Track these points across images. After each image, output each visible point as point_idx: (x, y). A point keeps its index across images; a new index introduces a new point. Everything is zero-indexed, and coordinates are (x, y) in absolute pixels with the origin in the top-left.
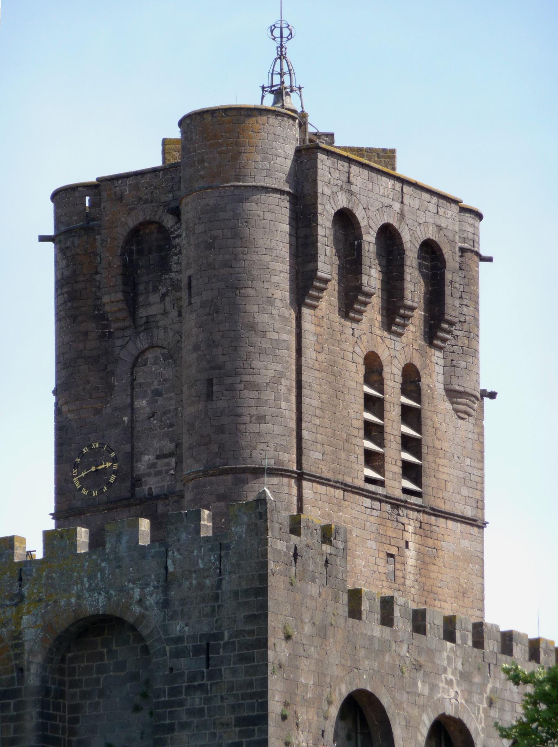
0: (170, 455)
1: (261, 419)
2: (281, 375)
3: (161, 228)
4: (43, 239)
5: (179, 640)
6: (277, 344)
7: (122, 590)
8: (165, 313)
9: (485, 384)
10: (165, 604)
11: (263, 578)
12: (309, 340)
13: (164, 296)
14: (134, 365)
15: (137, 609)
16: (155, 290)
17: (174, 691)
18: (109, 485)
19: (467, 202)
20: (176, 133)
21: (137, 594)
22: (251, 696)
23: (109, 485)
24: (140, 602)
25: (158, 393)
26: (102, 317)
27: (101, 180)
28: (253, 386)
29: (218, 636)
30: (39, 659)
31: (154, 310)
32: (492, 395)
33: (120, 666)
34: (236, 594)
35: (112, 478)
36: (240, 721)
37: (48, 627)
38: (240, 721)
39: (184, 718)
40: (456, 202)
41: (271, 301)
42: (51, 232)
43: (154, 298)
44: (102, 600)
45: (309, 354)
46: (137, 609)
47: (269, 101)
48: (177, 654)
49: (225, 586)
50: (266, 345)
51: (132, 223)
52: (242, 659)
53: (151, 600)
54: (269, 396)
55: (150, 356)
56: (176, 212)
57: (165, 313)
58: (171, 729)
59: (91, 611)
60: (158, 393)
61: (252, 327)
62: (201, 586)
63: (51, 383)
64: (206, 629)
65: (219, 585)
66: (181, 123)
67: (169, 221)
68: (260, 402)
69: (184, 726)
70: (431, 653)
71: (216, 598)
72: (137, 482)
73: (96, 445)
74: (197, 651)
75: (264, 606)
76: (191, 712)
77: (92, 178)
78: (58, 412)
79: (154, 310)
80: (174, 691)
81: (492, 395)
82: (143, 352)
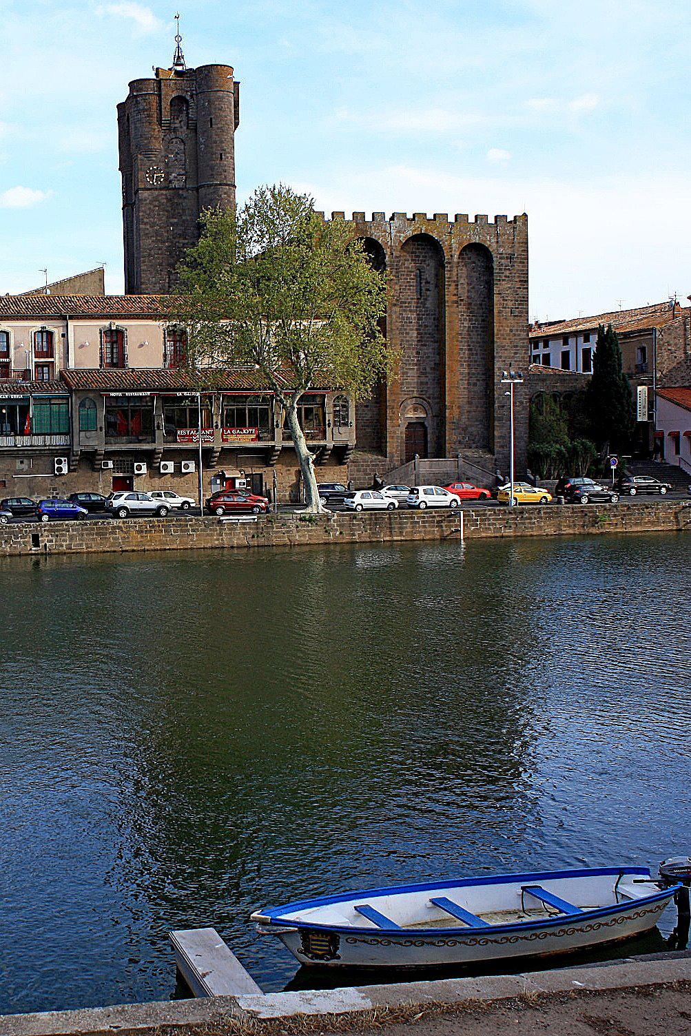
0: (182, 175)
5: (501, 254)
13: (180, 122)
16: (177, 119)
18: (161, 182)
22: (524, 274)
23: (161, 182)
30: (458, 253)
33: (469, 259)
34: (519, 243)
35: (162, 180)
36: (521, 281)
37: (460, 244)
38: (521, 281)
43: (177, 121)
48: (501, 258)
52: (520, 262)
53: (493, 241)
55: (174, 140)
59: (474, 241)
62: (508, 239)
69: (503, 280)
73: (155, 167)
76: (506, 276)
82: (173, 138)
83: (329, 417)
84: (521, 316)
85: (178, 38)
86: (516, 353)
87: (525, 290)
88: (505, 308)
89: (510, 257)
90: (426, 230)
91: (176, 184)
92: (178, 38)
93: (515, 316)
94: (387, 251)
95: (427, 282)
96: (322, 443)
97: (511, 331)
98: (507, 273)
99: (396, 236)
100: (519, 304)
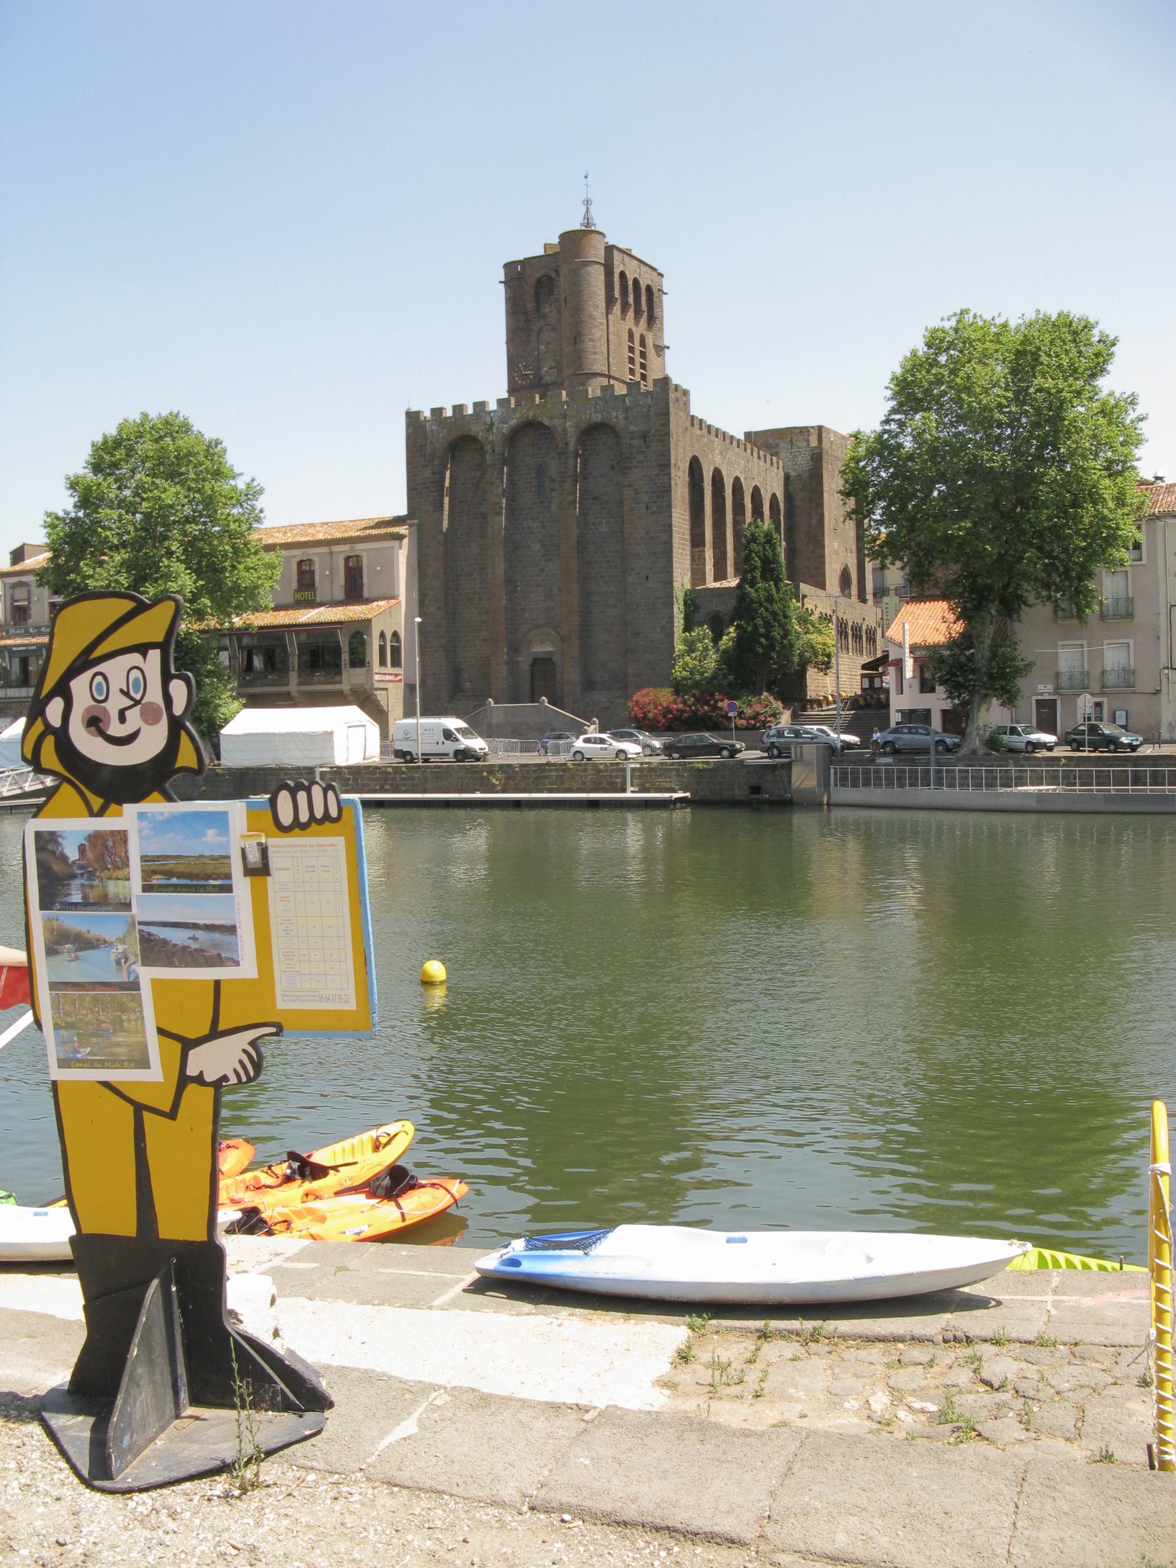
1: (595, 353)
2: (602, 336)
3: (550, 278)
4: (501, 282)
5: (632, 433)
6: (601, 323)
7: (609, 412)
8: (551, 311)
9: (666, 343)
10: (626, 418)
11: (668, 408)
12: (611, 322)
13: (551, 305)
14: (539, 332)
15: (615, 420)
17: (631, 453)
19: (660, 271)
20: (556, 241)
21: (614, 414)
24: (616, 417)
25: (548, 343)
26: (526, 313)
27: (525, 259)
28: (592, 340)
29: (649, 431)
31: (547, 310)
32: (668, 348)
34: (656, 415)
36: (659, 466)
38: (659, 466)
39: (636, 464)
40: (655, 270)
41: (598, 307)
42: (503, 280)
44: (600, 416)
45: (611, 328)
46: (615, 420)
47: (584, 228)
48: (632, 438)
49: (652, 411)
50: (596, 324)
51: (538, 275)
52: (661, 441)
54: (598, 344)
55: (545, 328)
56: (557, 271)
57: (551, 311)
58: (630, 468)
59: (595, 420)
60: (548, 343)
61: (591, 316)
63: (505, 340)
64: (643, 429)
65: (649, 411)
66: (560, 237)
67: (553, 275)
68: (595, 347)
69: (636, 467)
70: (713, 442)
71: (648, 416)
72: (541, 378)
74: (640, 436)
75: (669, 419)
76: (638, 462)
77: (521, 258)
78: (508, 350)
79: (547, 310)
80: (631, 453)
81: (668, 348)
83: (345, 657)
84: (660, 512)
85: (587, 203)
86: (655, 563)
87: (666, 477)
88: (639, 503)
89: (644, 436)
90: (534, 415)
91: (548, 379)
92: (587, 203)
93: (653, 513)
94: (488, 448)
95: (552, 481)
96: (338, 687)
97: (647, 533)
98: (640, 457)
99: (498, 428)
100: (658, 497)
